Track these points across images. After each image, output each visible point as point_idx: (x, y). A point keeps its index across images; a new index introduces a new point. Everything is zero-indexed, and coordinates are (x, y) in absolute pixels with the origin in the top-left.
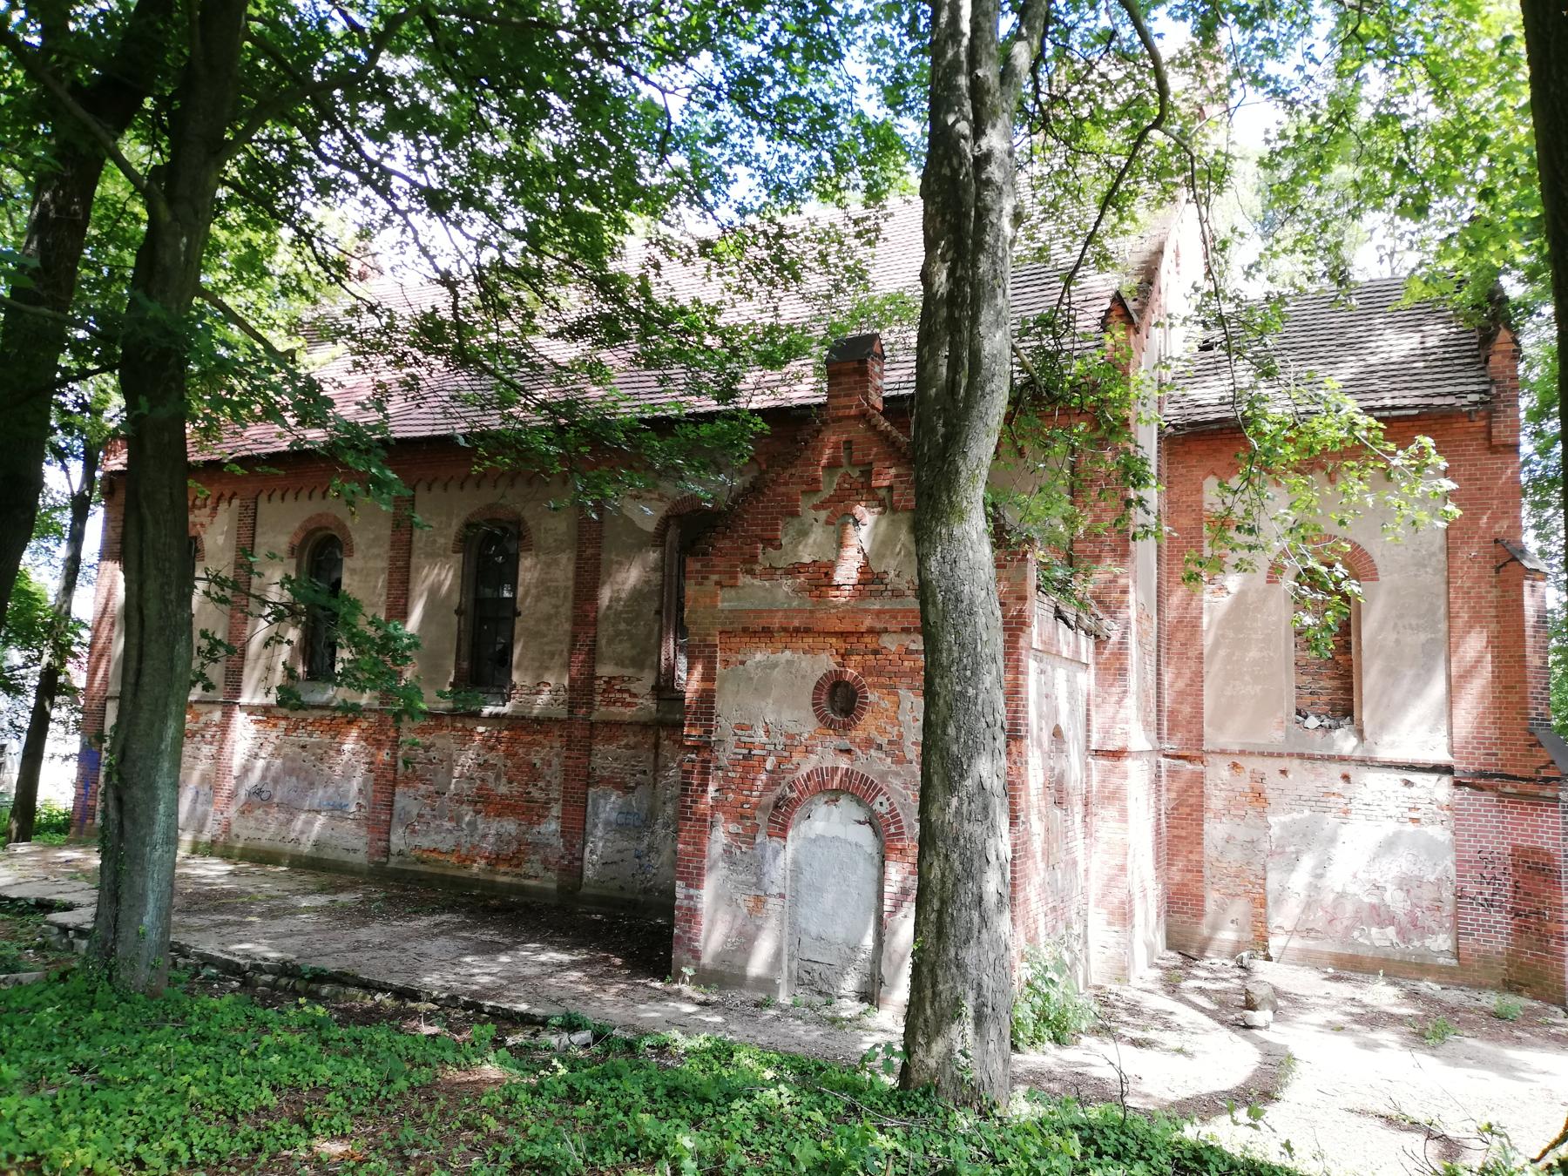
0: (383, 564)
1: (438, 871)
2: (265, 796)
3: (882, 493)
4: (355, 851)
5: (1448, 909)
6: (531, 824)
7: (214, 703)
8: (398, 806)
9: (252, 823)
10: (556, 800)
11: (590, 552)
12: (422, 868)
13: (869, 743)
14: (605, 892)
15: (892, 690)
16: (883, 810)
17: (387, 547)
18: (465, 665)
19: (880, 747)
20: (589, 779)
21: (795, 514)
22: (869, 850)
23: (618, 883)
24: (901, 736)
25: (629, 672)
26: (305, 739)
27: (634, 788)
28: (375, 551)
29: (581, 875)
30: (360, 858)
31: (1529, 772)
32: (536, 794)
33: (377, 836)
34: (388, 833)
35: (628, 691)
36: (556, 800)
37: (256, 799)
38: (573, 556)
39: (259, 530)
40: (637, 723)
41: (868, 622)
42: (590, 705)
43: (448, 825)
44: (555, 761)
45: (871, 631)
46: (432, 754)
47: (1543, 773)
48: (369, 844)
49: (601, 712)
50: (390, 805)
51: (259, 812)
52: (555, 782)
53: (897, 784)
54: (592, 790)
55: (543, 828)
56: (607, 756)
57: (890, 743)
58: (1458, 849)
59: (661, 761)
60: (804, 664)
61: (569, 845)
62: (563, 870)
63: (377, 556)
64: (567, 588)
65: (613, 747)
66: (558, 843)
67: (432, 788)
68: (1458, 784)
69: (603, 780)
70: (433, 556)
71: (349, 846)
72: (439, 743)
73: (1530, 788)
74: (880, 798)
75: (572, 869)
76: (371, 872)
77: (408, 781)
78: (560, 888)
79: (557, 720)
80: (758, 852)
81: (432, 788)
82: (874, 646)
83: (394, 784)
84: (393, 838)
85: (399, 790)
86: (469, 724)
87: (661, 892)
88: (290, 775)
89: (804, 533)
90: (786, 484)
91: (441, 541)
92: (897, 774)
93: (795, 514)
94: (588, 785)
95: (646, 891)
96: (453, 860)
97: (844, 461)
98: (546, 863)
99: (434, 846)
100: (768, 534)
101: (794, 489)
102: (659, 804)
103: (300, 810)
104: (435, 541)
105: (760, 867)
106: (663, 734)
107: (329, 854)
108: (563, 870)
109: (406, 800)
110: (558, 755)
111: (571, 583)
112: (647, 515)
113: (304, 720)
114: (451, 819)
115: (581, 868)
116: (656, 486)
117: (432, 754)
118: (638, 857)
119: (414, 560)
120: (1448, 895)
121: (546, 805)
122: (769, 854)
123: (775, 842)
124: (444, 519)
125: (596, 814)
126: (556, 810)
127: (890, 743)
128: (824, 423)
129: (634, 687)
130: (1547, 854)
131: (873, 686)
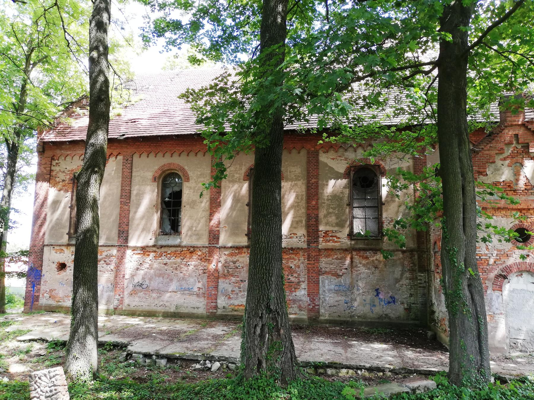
2: (144, 286)
4: (198, 308)
9: (137, 299)
10: (303, 282)
11: (313, 180)
12: (235, 313)
14: (331, 318)
18: (251, 227)
20: (320, 272)
21: (494, 162)
23: (336, 314)
25: (336, 229)
27: (341, 276)
29: (319, 312)
35: (336, 236)
36: (303, 282)
37: (138, 288)
38: (305, 181)
39: (134, 169)
40: (342, 249)
42: (317, 242)
46: (237, 265)
49: (322, 244)
50: (216, 287)
51: (141, 294)
52: (301, 274)
54: (321, 277)
55: (297, 293)
56: (324, 263)
59: (354, 264)
60: (503, 222)
62: (310, 310)
65: (330, 259)
66: (306, 299)
67: (238, 279)
69: (326, 273)
70: (233, 182)
71: (194, 306)
72: (241, 260)
75: (314, 310)
76: (208, 317)
77: (225, 276)
78: (310, 318)
79: (302, 249)
81: (238, 279)
83: (218, 278)
84: (219, 301)
87: (359, 317)
88: (159, 277)
89: (497, 170)
90: (489, 150)
91: (237, 176)
93: (494, 162)
95: (351, 317)
97: (514, 142)
98: (300, 308)
100: (482, 170)
101: (493, 152)
102: (355, 281)
103: (167, 292)
104: (234, 176)
106: (354, 253)
107: (183, 310)
108: (310, 310)
109: (223, 284)
110: (303, 263)
112: (341, 167)
115: (319, 309)
116: (343, 155)
117: (237, 265)
118: (346, 303)
122: (494, 297)
123: (497, 293)
124: (238, 167)
126: (304, 285)
128: (506, 127)
129: (338, 235)
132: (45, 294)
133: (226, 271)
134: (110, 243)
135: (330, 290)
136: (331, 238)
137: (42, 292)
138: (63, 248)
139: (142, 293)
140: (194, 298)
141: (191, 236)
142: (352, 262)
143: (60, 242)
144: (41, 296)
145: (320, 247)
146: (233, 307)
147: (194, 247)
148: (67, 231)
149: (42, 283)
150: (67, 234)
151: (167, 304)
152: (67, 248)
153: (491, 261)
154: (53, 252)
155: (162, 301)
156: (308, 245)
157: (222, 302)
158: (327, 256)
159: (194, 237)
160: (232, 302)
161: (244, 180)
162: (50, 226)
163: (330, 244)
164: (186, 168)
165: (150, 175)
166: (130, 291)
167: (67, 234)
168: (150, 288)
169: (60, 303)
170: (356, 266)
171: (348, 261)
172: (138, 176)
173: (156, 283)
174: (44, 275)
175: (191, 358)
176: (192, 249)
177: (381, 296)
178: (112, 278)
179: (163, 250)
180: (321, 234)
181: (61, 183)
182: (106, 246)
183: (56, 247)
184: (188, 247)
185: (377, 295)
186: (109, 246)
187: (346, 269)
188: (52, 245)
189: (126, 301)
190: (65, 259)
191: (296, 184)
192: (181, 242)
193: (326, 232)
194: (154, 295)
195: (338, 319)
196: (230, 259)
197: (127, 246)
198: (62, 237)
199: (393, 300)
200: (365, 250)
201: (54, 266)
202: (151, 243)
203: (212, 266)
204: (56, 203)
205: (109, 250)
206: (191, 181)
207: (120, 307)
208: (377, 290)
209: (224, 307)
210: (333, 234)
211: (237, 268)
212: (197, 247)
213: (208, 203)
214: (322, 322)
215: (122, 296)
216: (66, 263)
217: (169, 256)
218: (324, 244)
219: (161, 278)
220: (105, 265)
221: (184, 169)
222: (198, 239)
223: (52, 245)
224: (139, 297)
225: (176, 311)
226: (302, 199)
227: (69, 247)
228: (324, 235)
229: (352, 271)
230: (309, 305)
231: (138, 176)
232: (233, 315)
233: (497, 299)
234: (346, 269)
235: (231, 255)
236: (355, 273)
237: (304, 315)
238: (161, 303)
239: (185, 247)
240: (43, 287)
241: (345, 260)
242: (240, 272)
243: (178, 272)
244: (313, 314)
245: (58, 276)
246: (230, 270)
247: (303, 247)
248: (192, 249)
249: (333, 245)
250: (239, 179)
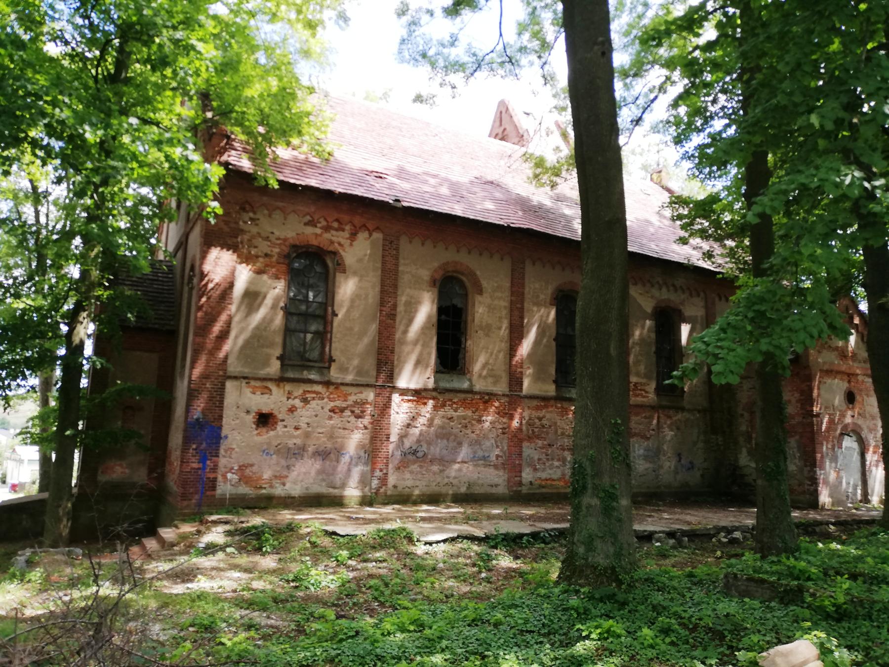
0: (504, 303)
1: (555, 491)
2: (420, 454)
4: (496, 486)
7: (368, 386)
8: (525, 454)
9: (408, 475)
12: (544, 490)
17: (507, 294)
25: (644, 381)
26: (450, 413)
28: (499, 294)
30: (502, 490)
33: (514, 474)
35: (644, 390)
37: (410, 457)
43: (556, 463)
46: (544, 422)
48: (509, 481)
51: (415, 467)
63: (500, 298)
65: (639, 418)
67: (545, 443)
69: (635, 435)
70: (538, 304)
77: (530, 439)
81: (545, 443)
83: (521, 441)
84: (524, 475)
85: (525, 444)
86: (565, 405)
88: (442, 439)
96: (562, 484)
99: (549, 477)
103: (455, 462)
104: (538, 297)
107: (477, 490)
109: (529, 451)
112: (648, 306)
113: (451, 400)
114: (559, 460)
117: (544, 422)
119: (526, 305)
132: (229, 475)
133: (530, 432)
134: (363, 380)
135: (639, 456)
137: (221, 469)
138: (270, 385)
139: (416, 466)
140: (491, 470)
141: (485, 377)
142: (658, 421)
143: (263, 373)
144: (220, 478)
146: (539, 482)
147: (488, 394)
148: (278, 352)
149: (222, 452)
150: (278, 358)
151: (455, 482)
152: (278, 386)
153: (836, 420)
154: (247, 391)
155: (448, 477)
157: (527, 475)
158: (637, 414)
159: (490, 380)
160: (539, 474)
161: (551, 304)
162: (240, 342)
163: (639, 400)
164: (478, 273)
165: (425, 274)
166: (397, 462)
167: (278, 358)
168: (430, 457)
169: (264, 491)
171: (655, 422)
172: (407, 272)
173: (438, 449)
174: (226, 437)
175: (704, 532)
176: (487, 397)
177: (683, 462)
178: (367, 441)
179: (448, 396)
181: (261, 259)
182: (352, 385)
183: (253, 383)
184: (484, 393)
185: (680, 461)
186: (362, 385)
187: (653, 430)
188: (245, 378)
189: (392, 480)
190: (272, 406)
192: (471, 385)
193: (636, 384)
194: (435, 468)
196: (535, 414)
197: (394, 387)
198: (266, 363)
199: (691, 466)
200: (669, 408)
201: (250, 419)
202: (431, 384)
203: (515, 423)
204: (252, 297)
205: (361, 393)
206: (485, 295)
207: (382, 490)
208: (679, 455)
209: (531, 483)
210: (643, 387)
211: (543, 427)
212: (496, 395)
213: (507, 331)
215: (385, 471)
216: (275, 412)
217: (455, 406)
219: (445, 441)
220: (352, 419)
221: (475, 274)
222: (495, 383)
223: (245, 378)
224: (411, 472)
225: (468, 492)
227: (282, 384)
231: (407, 272)
232: (542, 494)
234: (653, 430)
235: (538, 408)
236: (661, 435)
238: (446, 480)
239: (479, 393)
240: (223, 461)
241: (653, 419)
242: (547, 433)
243: (469, 431)
245: (259, 439)
246: (536, 430)
248: (487, 397)
250: (545, 302)
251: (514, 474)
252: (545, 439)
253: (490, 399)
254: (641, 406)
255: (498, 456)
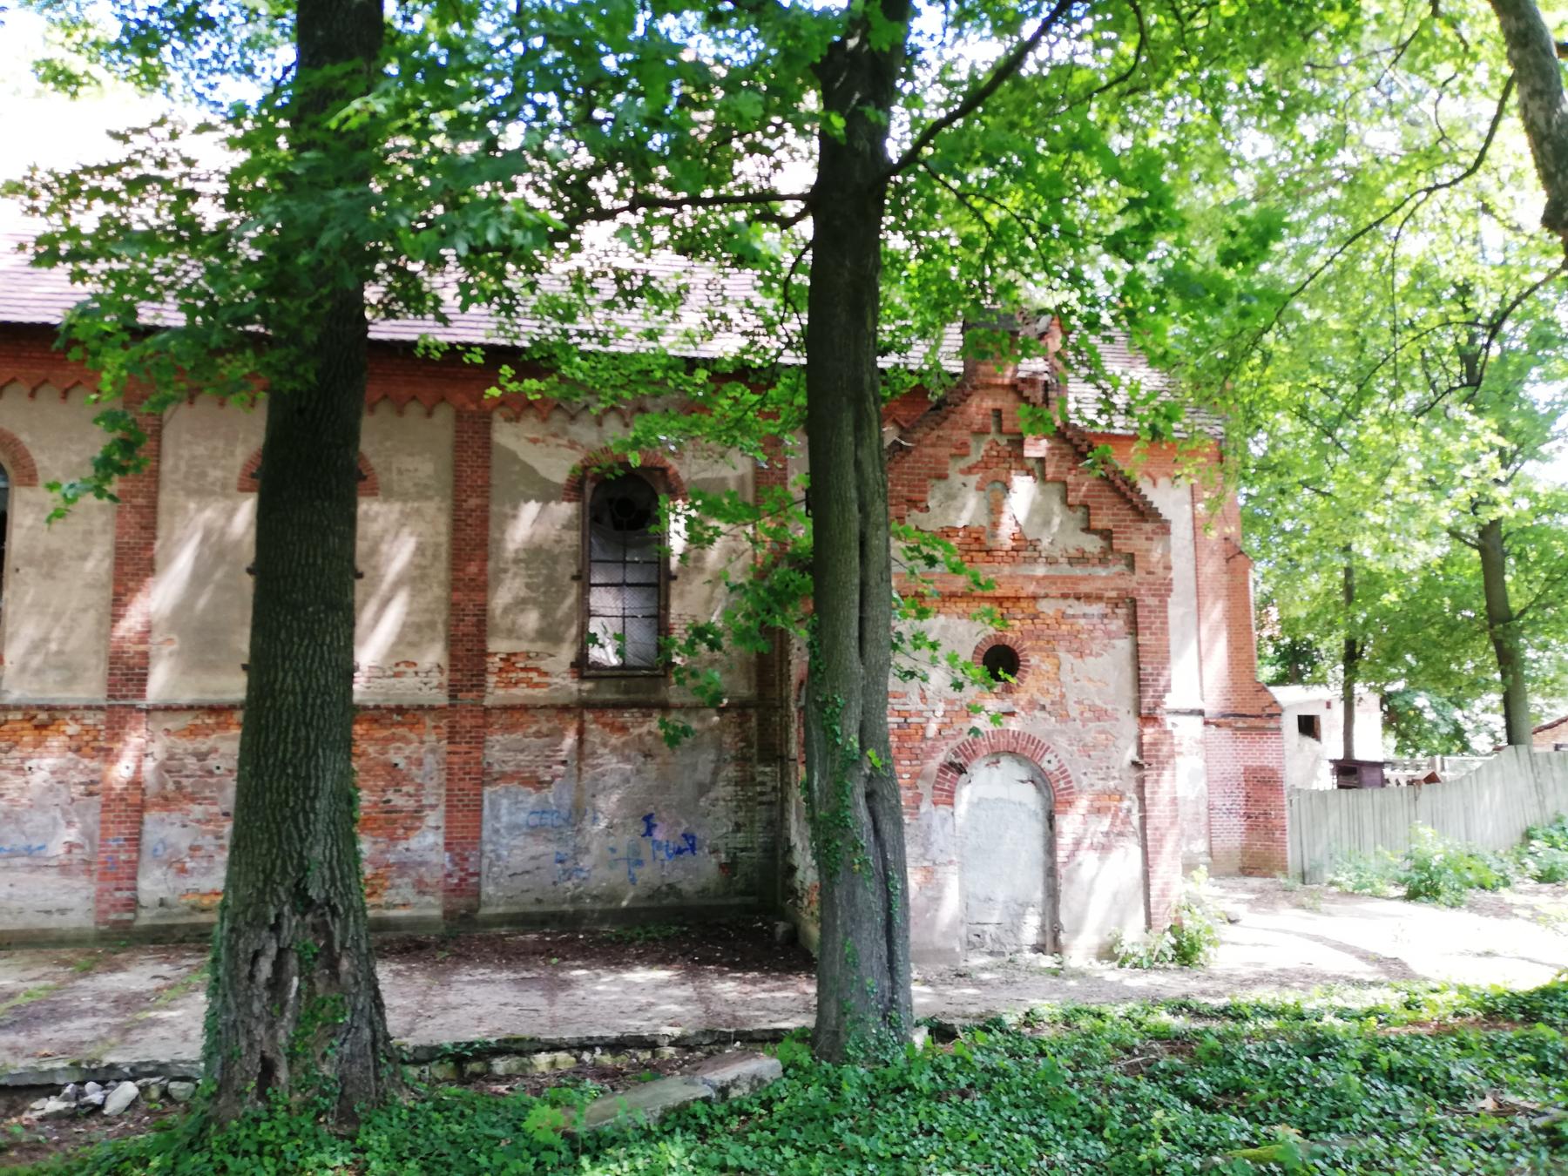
3: (1031, 464)
4: (63, 911)
5: (1204, 819)
6: (393, 839)
11: (473, 502)
13: (1033, 704)
14: (515, 909)
15: (1051, 653)
16: (1051, 768)
19: (1043, 708)
20: (484, 777)
21: (943, 477)
22: (1033, 807)
23: (532, 896)
24: (1063, 696)
25: (539, 646)
27: (550, 783)
29: (478, 895)
31: (1259, 712)
32: (398, 801)
33: (113, 884)
34: (133, 878)
35: (536, 670)
36: (433, 807)
38: (447, 504)
40: (553, 706)
41: (1031, 588)
42: (480, 686)
44: (430, 760)
45: (1035, 598)
46: (212, 762)
47: (1268, 711)
49: (496, 694)
50: (135, 840)
52: (428, 784)
53: (1062, 742)
54: (487, 791)
55: (414, 843)
56: (500, 749)
57: (1053, 703)
58: (1208, 772)
59: (587, 749)
60: (960, 629)
61: (460, 860)
62: (456, 890)
64: (438, 545)
65: (517, 736)
66: (442, 858)
67: (215, 809)
68: (1206, 723)
69: (504, 777)
70: (202, 492)
71: (48, 905)
73: (1257, 722)
74: (1048, 757)
77: (166, 802)
78: (448, 914)
79: (432, 708)
80: (924, 822)
81: (215, 809)
82: (1031, 610)
83: (141, 808)
85: (150, 817)
87: (595, 898)
89: (951, 496)
90: (933, 445)
91: (215, 474)
92: (1063, 732)
93: (943, 477)
94: (483, 784)
95: (575, 899)
97: (993, 429)
98: (421, 887)
100: (915, 496)
101: (944, 452)
102: (587, 797)
104: (203, 475)
105: (927, 837)
106: (589, 716)
109: (161, 830)
110: (433, 751)
111: (443, 539)
112: (558, 466)
115: (478, 885)
116: (565, 432)
117: (212, 762)
118: (561, 862)
119: (164, 499)
120: (1203, 809)
121: (417, 813)
122: (936, 822)
123: (943, 810)
124: (221, 444)
125: (497, 818)
126: (434, 818)
127: (1053, 703)
128: (975, 388)
129: (544, 665)
130: (1272, 770)
131: (1033, 649)
133: (170, 786)
135: (513, 828)
136: (522, 675)
140: (51, 879)
141: (39, 672)
142: (581, 741)
145: (488, 701)
146: (193, 899)
147: (50, 708)
153: (932, 730)
156: (452, 696)
157: (153, 885)
158: (508, 729)
159: (52, 677)
160: (190, 882)
161: (242, 489)
163: (520, 693)
164: (25, 438)
170: (593, 753)
171: (570, 741)
175: (31, 1080)
176: (43, 716)
177: (659, 835)
180: (495, 663)
184: (29, 707)
185: (649, 832)
187: (564, 763)
191: (418, 511)
193: (509, 658)
195: (534, 909)
196: (185, 745)
199: (690, 843)
200: (618, 706)
203: (122, 771)
209: (162, 903)
210: (531, 664)
211: (210, 773)
212: (65, 709)
213: (107, 564)
214: (489, 922)
218: (500, 692)
221: (14, 442)
222: (69, 682)
226: (435, 557)
228: (501, 665)
229: (580, 769)
230: (449, 875)
232: (194, 927)
233: (943, 826)
234: (564, 763)
235: (193, 732)
236: (588, 774)
237: (431, 908)
239: (17, 708)
241: (563, 737)
244: (462, 901)
246: (185, 782)
247: (437, 704)
249: (526, 697)
250: (224, 486)
251: (113, 884)
252: (214, 802)
253: (53, 720)
254: (517, 712)
255: (71, 846)
